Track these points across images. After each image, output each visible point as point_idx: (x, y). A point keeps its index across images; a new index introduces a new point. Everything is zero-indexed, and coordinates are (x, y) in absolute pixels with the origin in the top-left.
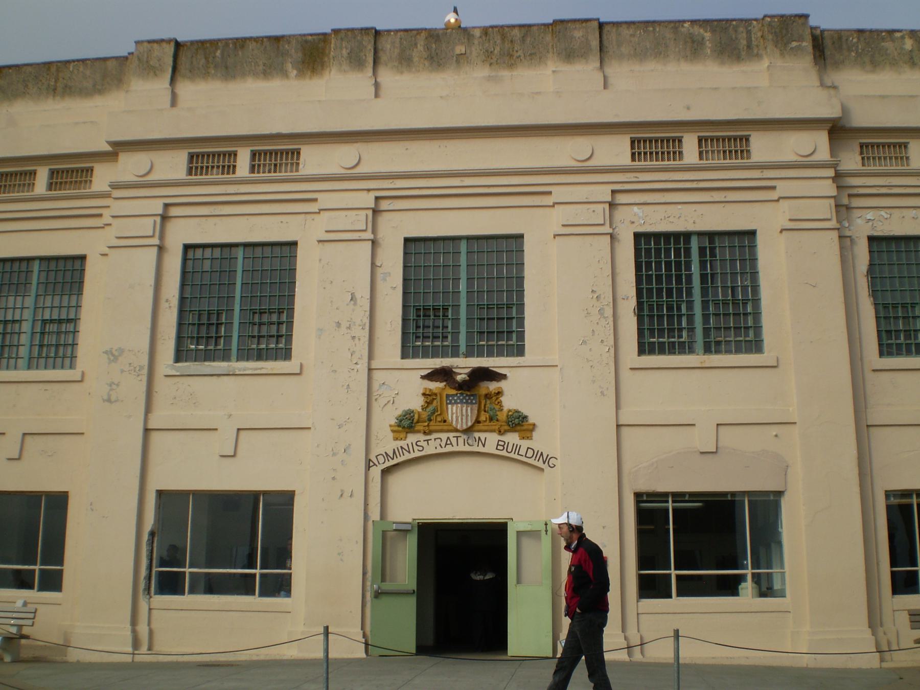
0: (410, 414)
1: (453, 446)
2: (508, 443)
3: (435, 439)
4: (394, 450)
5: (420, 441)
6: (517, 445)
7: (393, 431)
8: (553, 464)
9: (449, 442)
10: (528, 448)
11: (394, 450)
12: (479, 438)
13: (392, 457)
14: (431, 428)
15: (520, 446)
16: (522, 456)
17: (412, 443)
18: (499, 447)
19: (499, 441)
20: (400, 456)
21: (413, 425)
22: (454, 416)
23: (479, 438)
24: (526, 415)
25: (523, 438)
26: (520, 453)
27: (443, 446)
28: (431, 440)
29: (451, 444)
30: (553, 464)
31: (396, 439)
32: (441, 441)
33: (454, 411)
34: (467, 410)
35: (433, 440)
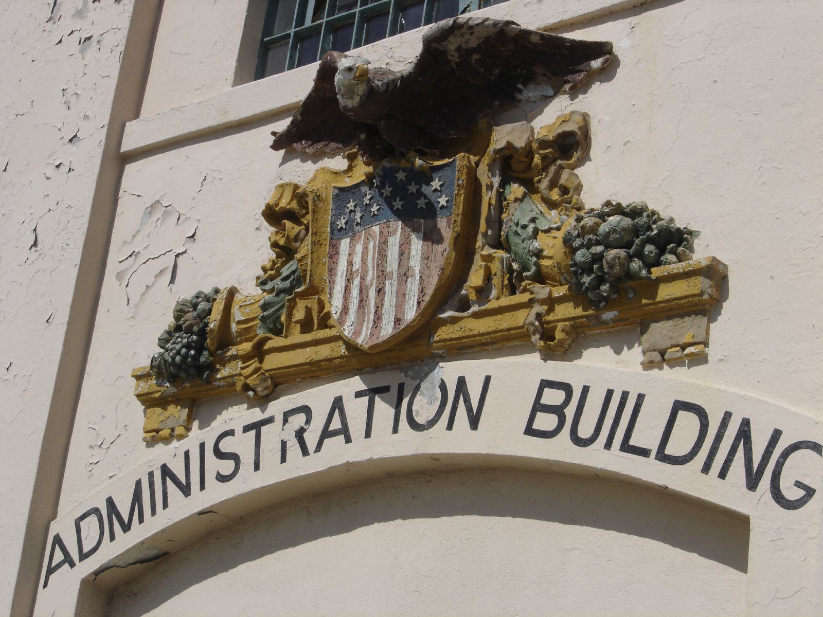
0: (195, 306)
1: (348, 440)
2: (586, 390)
3: (287, 416)
4: (139, 483)
5: (231, 433)
6: (625, 395)
7: (148, 401)
8: (799, 484)
9: (336, 424)
10: (679, 406)
11: (139, 483)
12: (462, 382)
13: (126, 520)
14: (272, 362)
15: (641, 397)
16: (644, 452)
17: (202, 446)
18: (546, 421)
19: (546, 384)
20: (154, 512)
21: (205, 357)
22: (357, 282)
23: (462, 382)
24: (680, 224)
25: (663, 353)
26: (632, 442)
27: (312, 443)
28: (270, 420)
29: (344, 431)
30: (799, 484)
31: (154, 437)
32: (308, 422)
33: (357, 260)
34: (403, 253)
35: (279, 419)
